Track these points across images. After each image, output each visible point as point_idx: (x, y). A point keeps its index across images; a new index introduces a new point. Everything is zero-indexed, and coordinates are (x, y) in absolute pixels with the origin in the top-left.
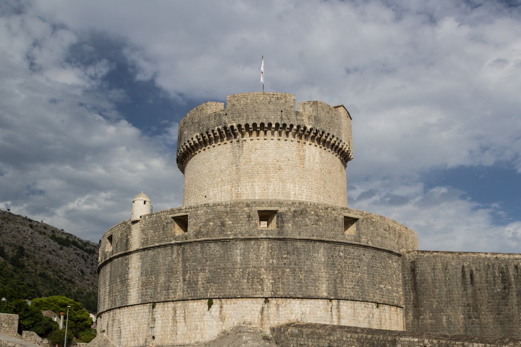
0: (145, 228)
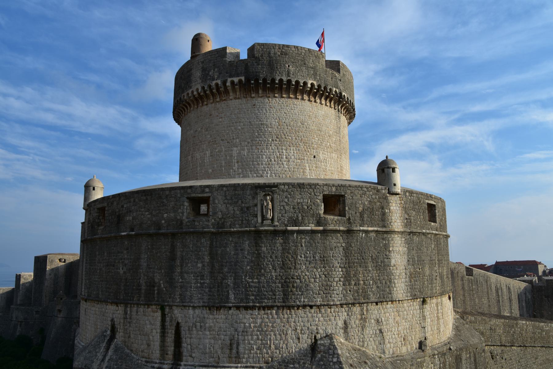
0: (407, 206)
